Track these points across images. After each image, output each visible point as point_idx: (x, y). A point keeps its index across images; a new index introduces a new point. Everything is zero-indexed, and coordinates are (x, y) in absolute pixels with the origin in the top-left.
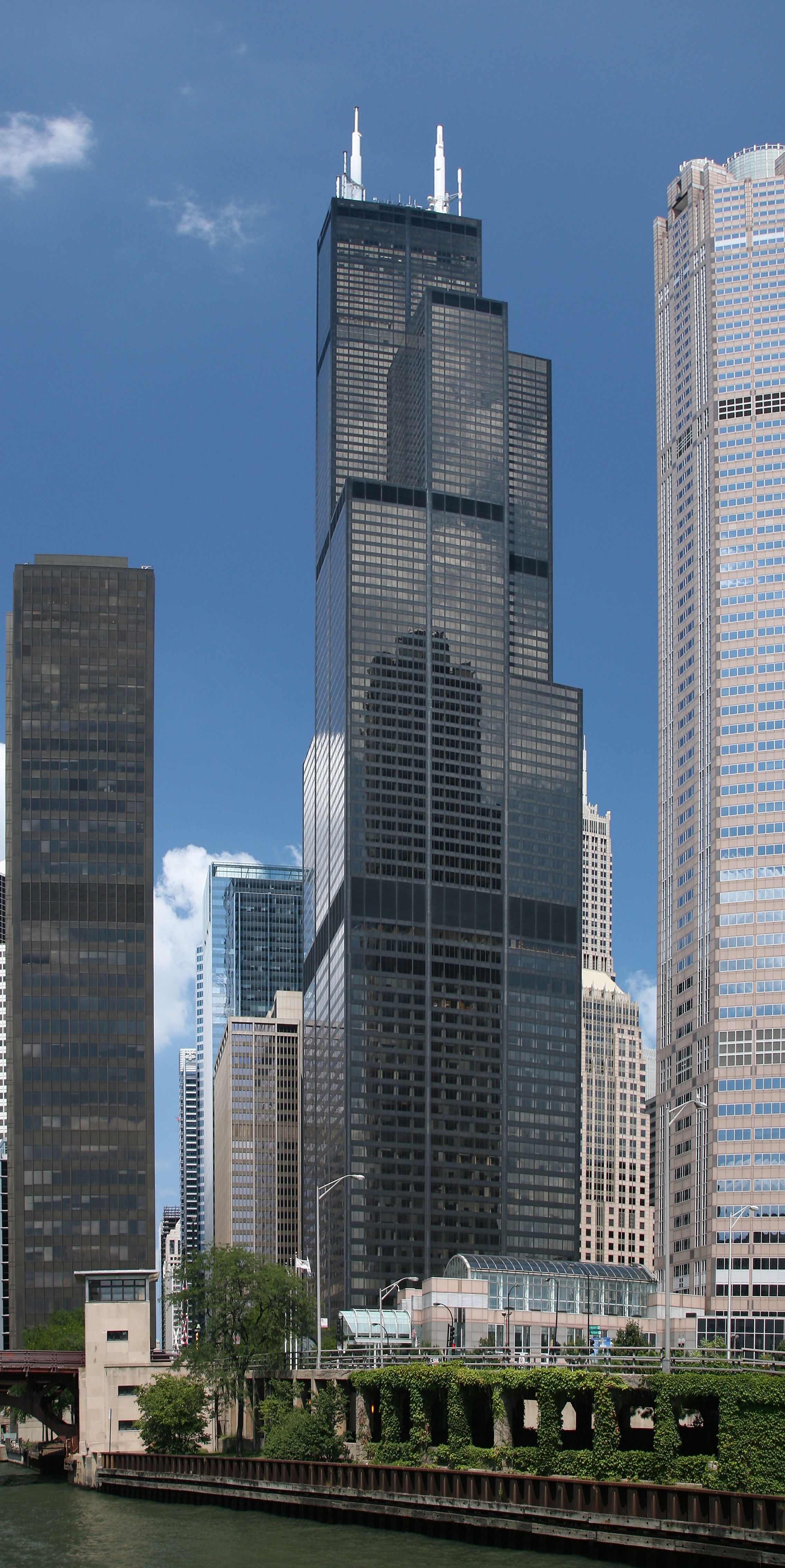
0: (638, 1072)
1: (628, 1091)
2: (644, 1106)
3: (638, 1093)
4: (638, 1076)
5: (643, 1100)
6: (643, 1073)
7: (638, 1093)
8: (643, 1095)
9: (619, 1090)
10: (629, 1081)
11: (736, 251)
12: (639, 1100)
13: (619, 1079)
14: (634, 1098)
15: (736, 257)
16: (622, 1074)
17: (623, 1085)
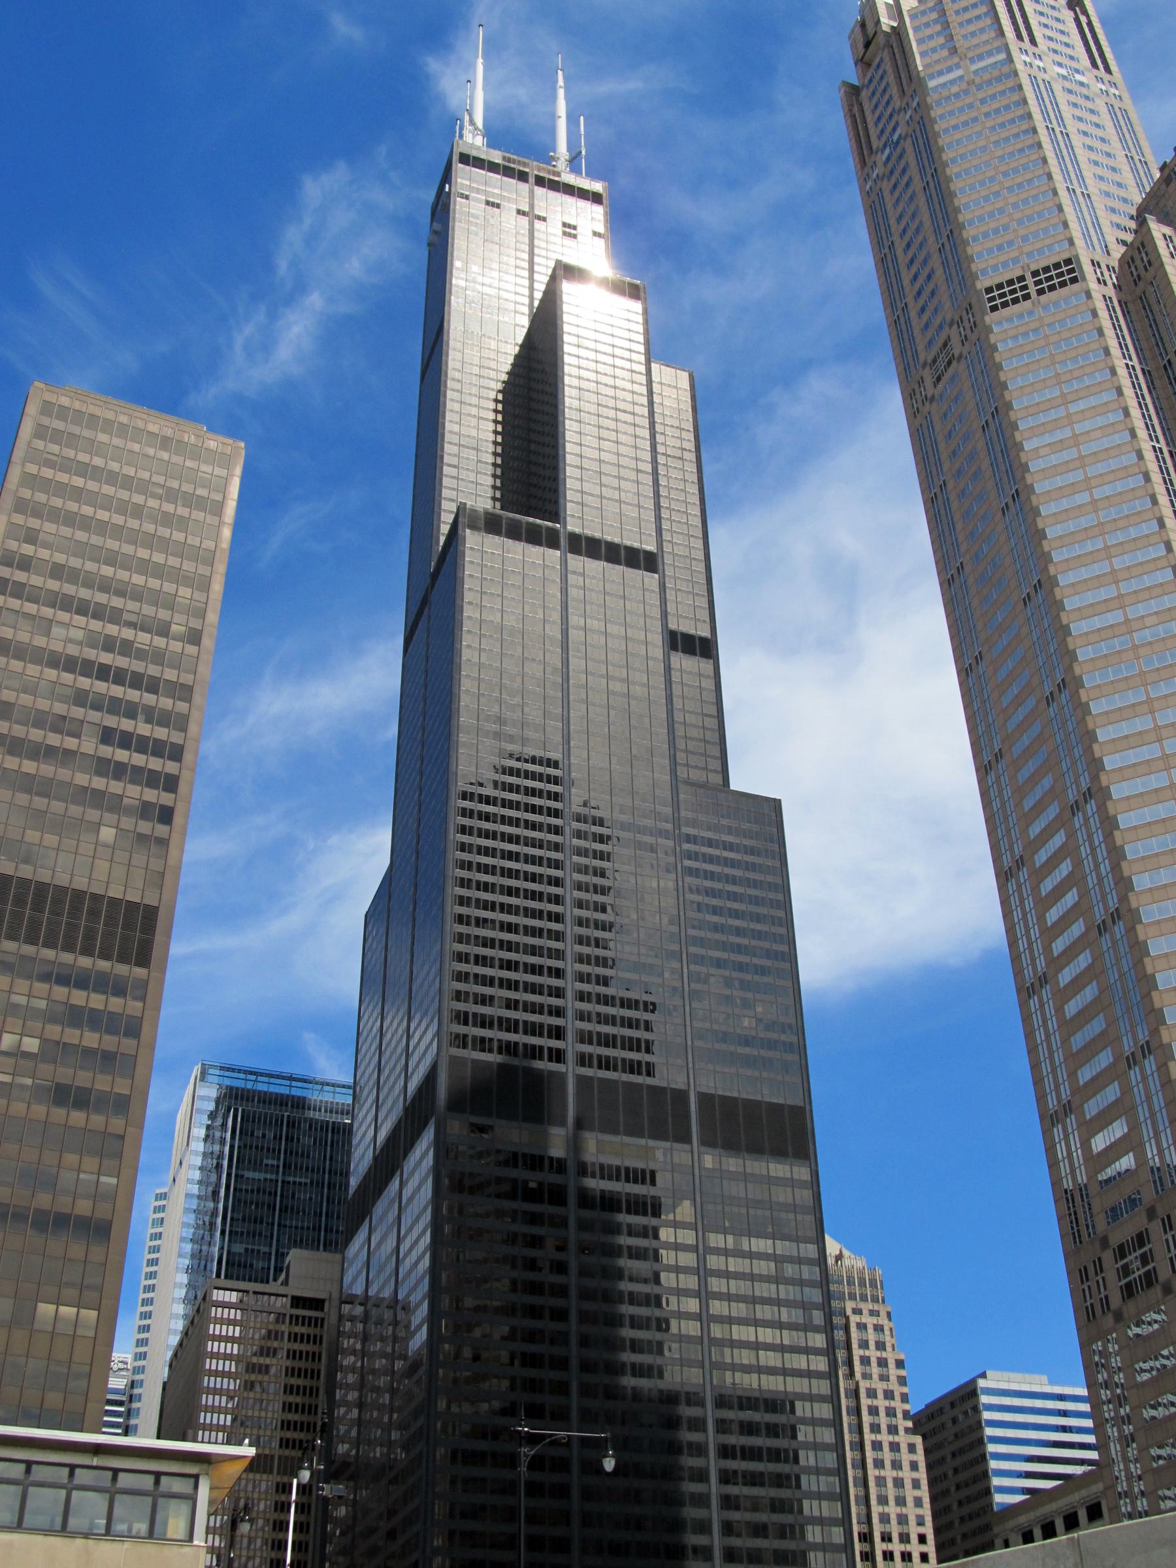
0: (893, 1371)
1: (881, 1403)
2: (910, 1424)
3: (897, 1404)
4: (893, 1378)
5: (906, 1415)
6: (903, 1373)
7: (897, 1404)
8: (907, 1407)
9: (865, 1402)
10: (880, 1387)
11: (954, 89)
12: (900, 1415)
13: (864, 1385)
14: (891, 1412)
15: (957, 95)
16: (866, 1376)
17: (872, 1393)
